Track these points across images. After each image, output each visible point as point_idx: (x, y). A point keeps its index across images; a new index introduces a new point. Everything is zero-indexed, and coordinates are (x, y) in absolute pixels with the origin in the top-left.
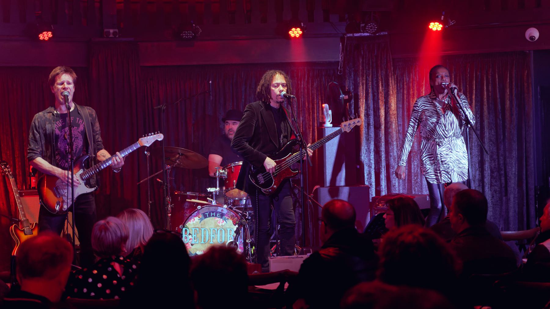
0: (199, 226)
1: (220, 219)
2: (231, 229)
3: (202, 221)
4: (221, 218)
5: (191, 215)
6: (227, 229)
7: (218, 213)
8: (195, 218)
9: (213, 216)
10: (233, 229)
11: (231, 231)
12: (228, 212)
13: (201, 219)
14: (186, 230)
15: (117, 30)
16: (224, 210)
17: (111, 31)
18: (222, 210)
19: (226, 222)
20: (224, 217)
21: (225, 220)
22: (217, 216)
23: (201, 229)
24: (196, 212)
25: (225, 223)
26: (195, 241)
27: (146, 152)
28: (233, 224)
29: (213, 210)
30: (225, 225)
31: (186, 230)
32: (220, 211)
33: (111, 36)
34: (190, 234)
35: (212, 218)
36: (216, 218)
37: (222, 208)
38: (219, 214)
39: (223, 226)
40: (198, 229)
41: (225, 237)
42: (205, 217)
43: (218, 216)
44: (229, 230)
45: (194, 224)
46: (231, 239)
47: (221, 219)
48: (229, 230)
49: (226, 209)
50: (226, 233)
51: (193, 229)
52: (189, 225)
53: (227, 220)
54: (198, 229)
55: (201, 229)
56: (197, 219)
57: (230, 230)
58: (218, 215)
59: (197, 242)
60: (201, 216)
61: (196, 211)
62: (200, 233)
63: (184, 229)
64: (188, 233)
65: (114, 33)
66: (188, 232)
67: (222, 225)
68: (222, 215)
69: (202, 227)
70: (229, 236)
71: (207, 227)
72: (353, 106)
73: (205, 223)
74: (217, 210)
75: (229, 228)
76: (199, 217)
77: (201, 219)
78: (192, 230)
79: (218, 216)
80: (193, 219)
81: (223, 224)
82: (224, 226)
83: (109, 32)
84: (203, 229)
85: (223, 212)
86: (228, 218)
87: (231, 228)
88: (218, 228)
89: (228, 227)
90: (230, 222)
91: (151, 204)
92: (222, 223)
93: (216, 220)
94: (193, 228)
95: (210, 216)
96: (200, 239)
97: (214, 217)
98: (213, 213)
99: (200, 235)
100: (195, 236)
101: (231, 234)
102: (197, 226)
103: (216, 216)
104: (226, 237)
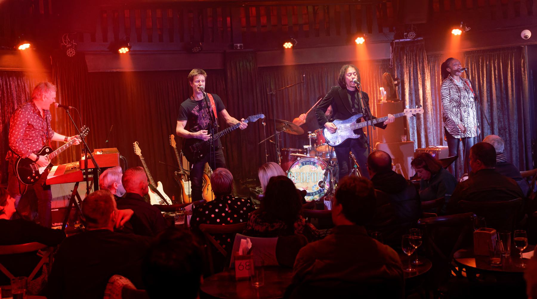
0: (299, 171)
3: (301, 168)
4: (314, 165)
5: (294, 164)
8: (296, 166)
9: (308, 164)
13: (301, 167)
14: (290, 174)
15: (242, 44)
16: (315, 159)
17: (239, 45)
18: (314, 160)
20: (316, 165)
21: (316, 166)
23: (301, 173)
24: (297, 162)
26: (297, 181)
27: (263, 123)
29: (309, 160)
31: (290, 174)
32: (313, 161)
33: (239, 48)
34: (293, 177)
35: (307, 165)
36: (310, 165)
37: (314, 159)
40: (298, 173)
42: (303, 165)
44: (319, 173)
45: (295, 170)
47: (314, 166)
48: (319, 173)
49: (317, 159)
50: (317, 176)
51: (295, 173)
52: (293, 170)
54: (298, 173)
55: (301, 173)
56: (297, 166)
57: (320, 173)
59: (298, 182)
60: (300, 164)
61: (297, 161)
62: (300, 176)
63: (289, 173)
64: (292, 176)
65: (240, 46)
66: (292, 175)
67: (314, 170)
68: (314, 164)
69: (301, 171)
70: (319, 177)
71: (304, 172)
72: (401, 88)
73: (303, 169)
76: (299, 165)
77: (301, 167)
78: (295, 174)
80: (295, 167)
81: (315, 169)
83: (237, 45)
84: (302, 173)
85: (315, 161)
88: (312, 172)
89: (318, 171)
90: (320, 168)
91: (267, 157)
92: (314, 169)
93: (311, 166)
94: (296, 172)
95: (306, 164)
96: (300, 180)
97: (309, 165)
98: (308, 162)
99: (300, 177)
100: (297, 177)
101: (321, 176)
102: (298, 171)
103: (310, 164)
104: (317, 178)
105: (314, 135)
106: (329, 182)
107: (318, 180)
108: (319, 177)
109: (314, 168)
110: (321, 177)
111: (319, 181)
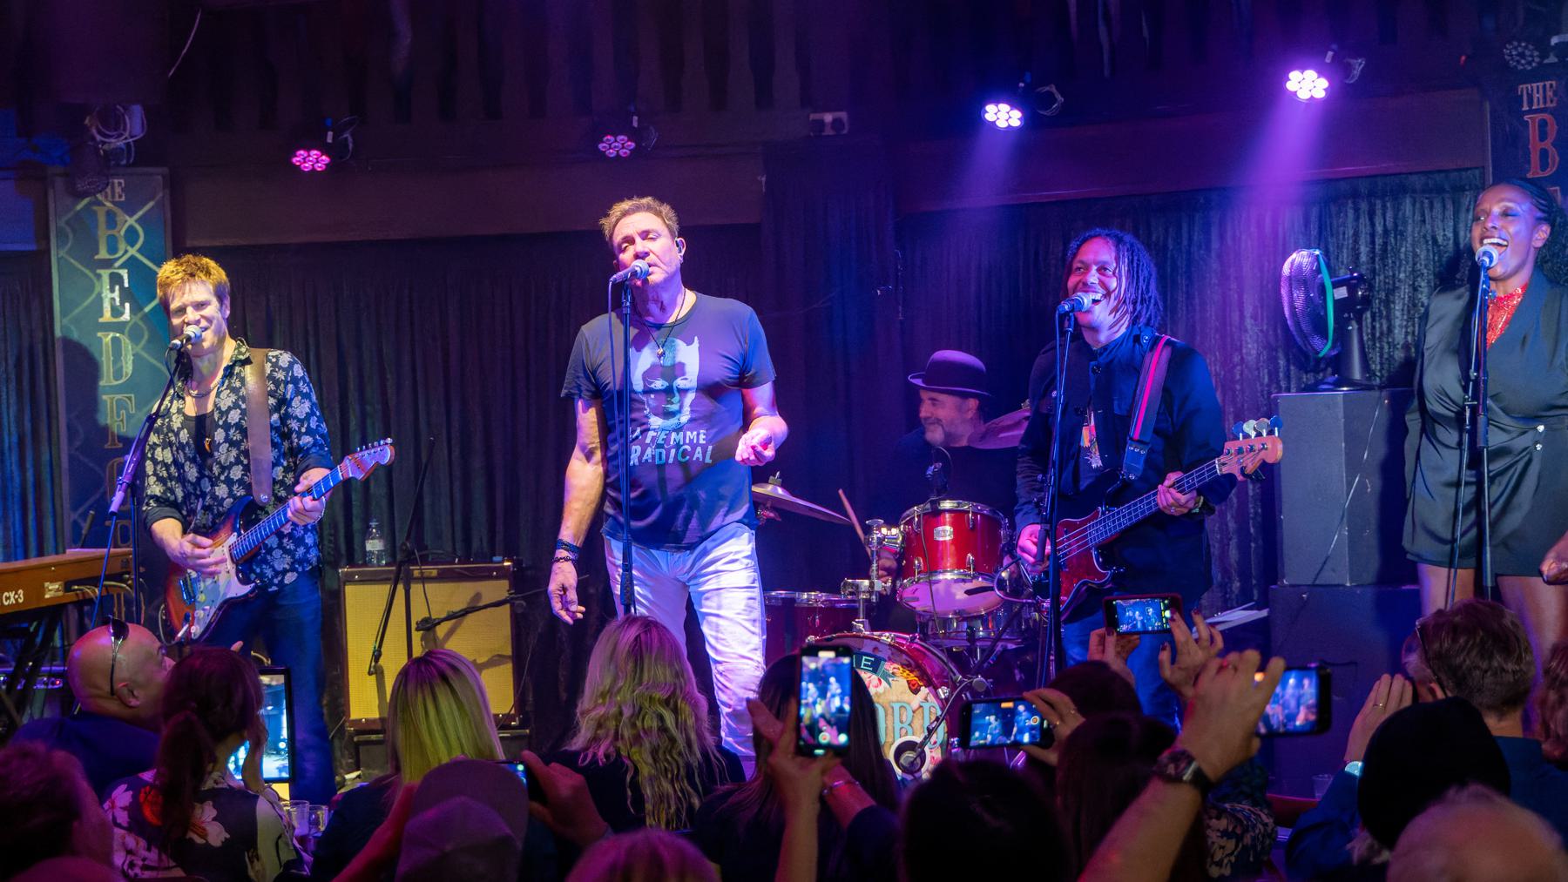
1: (869, 674)
2: (904, 705)
4: (875, 671)
6: (893, 705)
7: (864, 657)
10: (909, 704)
11: (903, 710)
12: (892, 654)
18: (875, 649)
19: (889, 684)
21: (886, 676)
22: (862, 667)
25: (885, 688)
28: (910, 688)
30: (884, 692)
32: (870, 652)
38: (866, 660)
39: (880, 694)
41: (886, 728)
43: (865, 665)
46: (906, 734)
50: (890, 717)
53: (890, 679)
57: (901, 707)
58: (863, 662)
70: (898, 725)
74: (860, 649)
75: (898, 702)
79: (865, 665)
82: (882, 697)
85: (879, 654)
86: (895, 670)
87: (904, 702)
89: (894, 698)
92: (876, 687)
101: (904, 719)
104: (890, 728)
105: (892, 534)
106: (941, 745)
107: (891, 740)
108: (898, 725)
109: (876, 682)
110: (905, 725)
111: (898, 742)
